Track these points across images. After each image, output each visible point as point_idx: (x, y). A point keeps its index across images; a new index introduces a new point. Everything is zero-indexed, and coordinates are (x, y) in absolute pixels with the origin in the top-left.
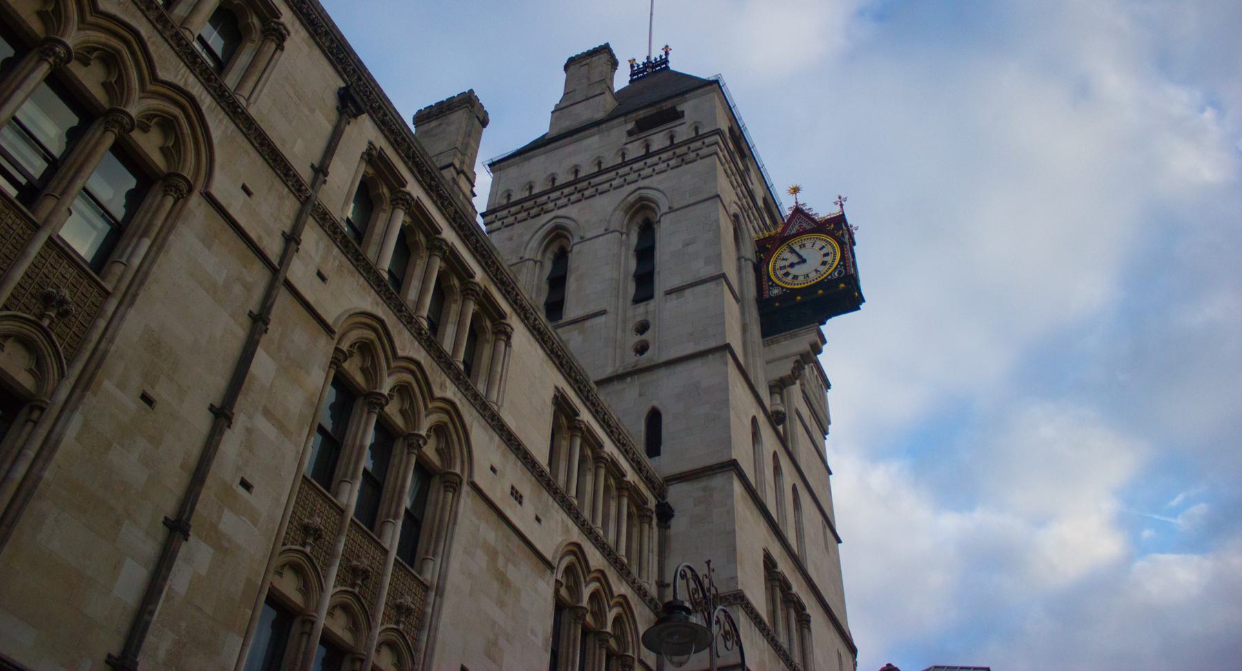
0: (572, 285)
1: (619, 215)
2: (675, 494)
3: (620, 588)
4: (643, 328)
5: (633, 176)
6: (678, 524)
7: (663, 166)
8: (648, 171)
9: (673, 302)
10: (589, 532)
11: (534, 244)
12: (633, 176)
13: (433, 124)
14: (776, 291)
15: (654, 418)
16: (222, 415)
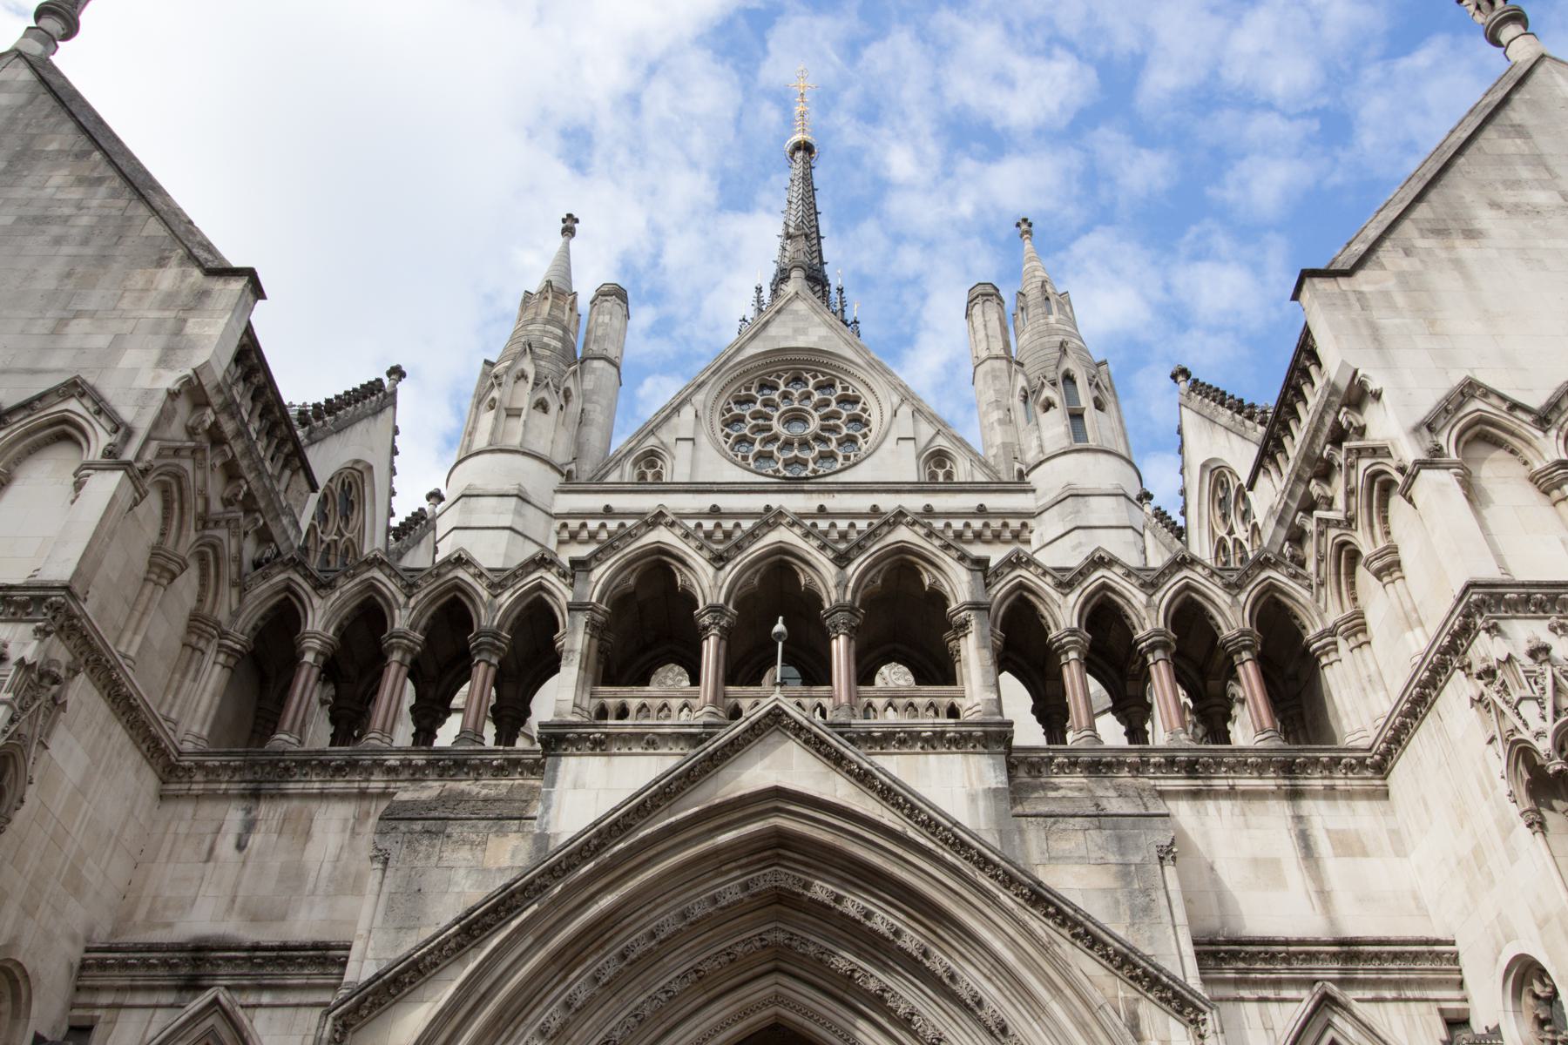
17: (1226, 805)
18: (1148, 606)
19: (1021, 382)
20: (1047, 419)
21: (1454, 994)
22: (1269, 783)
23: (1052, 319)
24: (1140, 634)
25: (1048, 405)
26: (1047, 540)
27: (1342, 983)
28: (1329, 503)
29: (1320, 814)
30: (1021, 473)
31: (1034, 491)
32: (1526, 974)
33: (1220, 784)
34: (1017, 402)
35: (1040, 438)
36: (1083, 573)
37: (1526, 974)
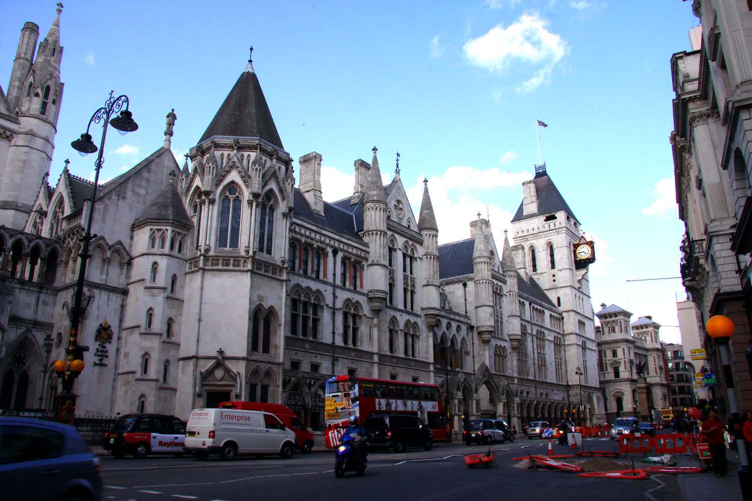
0: (538, 263)
1: (545, 245)
2: (564, 315)
3: (559, 336)
4: (554, 276)
5: (547, 235)
6: (565, 320)
7: (553, 234)
8: (550, 234)
9: (560, 273)
10: (555, 332)
11: (527, 250)
12: (547, 235)
13: (515, 252)
14: (578, 259)
15: (559, 299)
16: (533, 353)
17: (25, 291)
18: (28, 246)
19: (31, 79)
20: (35, 99)
21: (50, 332)
22: (36, 290)
23: (52, 59)
24: (23, 252)
25: (37, 95)
26: (17, 144)
27: (32, 327)
28: (72, 239)
29: (43, 297)
30: (17, 113)
31: (19, 124)
32: (60, 334)
33: (26, 288)
34: (27, 84)
35: (29, 106)
36: (17, 235)
37: (60, 334)
